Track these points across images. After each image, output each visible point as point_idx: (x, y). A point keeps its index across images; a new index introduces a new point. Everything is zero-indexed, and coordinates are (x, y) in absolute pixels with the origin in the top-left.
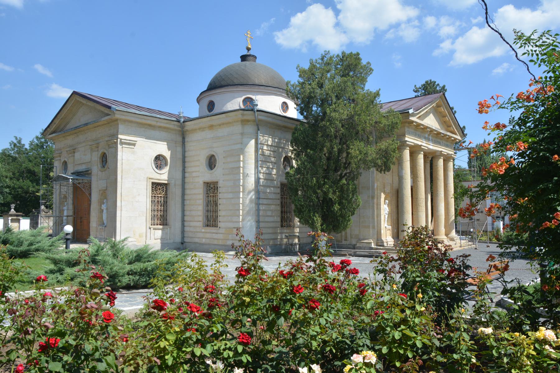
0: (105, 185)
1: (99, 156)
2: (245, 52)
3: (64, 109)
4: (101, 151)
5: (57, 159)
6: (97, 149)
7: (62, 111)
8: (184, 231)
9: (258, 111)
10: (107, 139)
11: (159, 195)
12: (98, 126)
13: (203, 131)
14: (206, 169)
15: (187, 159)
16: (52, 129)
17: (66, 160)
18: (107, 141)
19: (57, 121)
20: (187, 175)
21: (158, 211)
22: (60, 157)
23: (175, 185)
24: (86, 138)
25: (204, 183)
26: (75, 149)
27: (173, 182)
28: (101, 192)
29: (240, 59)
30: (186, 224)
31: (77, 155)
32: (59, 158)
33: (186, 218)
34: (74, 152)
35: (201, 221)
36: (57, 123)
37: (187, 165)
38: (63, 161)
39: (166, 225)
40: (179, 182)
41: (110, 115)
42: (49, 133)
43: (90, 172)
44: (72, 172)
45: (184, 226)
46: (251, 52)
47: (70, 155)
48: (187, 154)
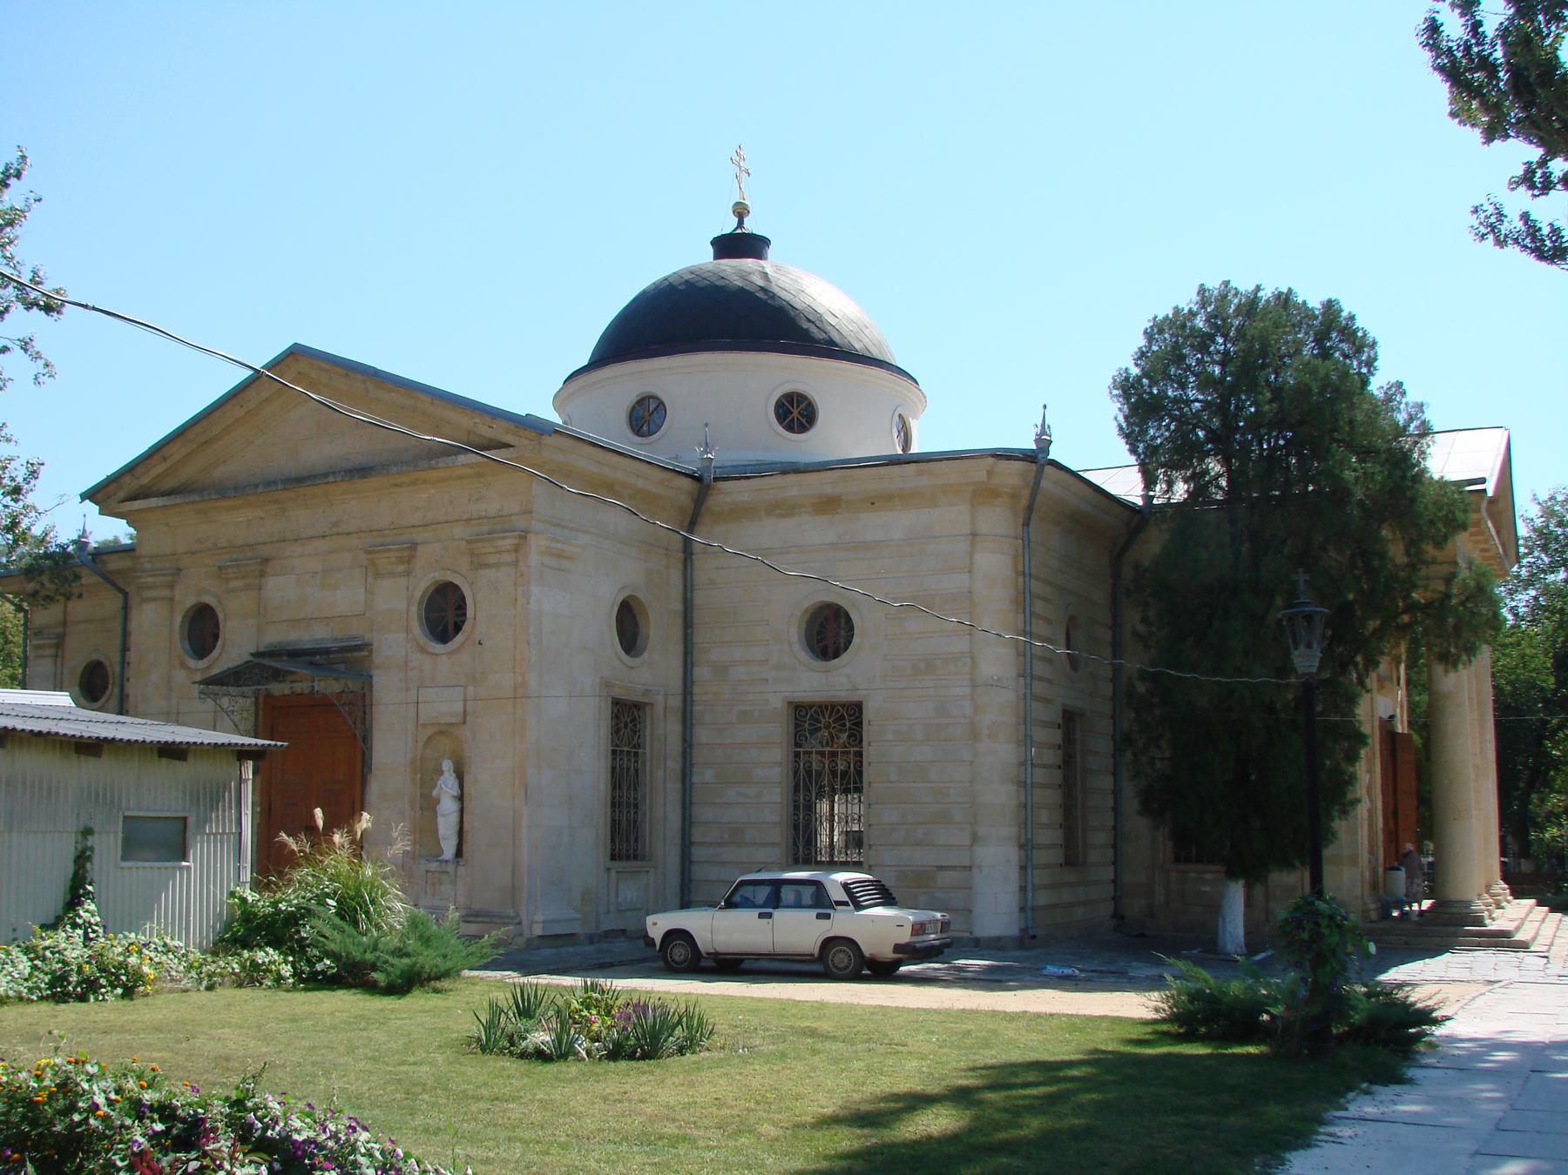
0: (459, 707)
1: (418, 595)
2: (728, 225)
3: (228, 406)
4: (423, 583)
5: (149, 594)
6: (402, 568)
7: (217, 414)
8: (690, 880)
9: (1054, 463)
10: (460, 531)
11: (626, 749)
12: (413, 483)
13: (783, 516)
14: (804, 655)
15: (697, 615)
16: (145, 480)
17: (208, 599)
18: (470, 542)
19: (178, 453)
20: (701, 673)
21: (628, 805)
22: (171, 586)
23: (666, 707)
24: (335, 524)
25: (790, 703)
26: (266, 560)
27: (660, 699)
28: (430, 731)
29: (710, 251)
30: (697, 853)
31: (279, 588)
32: (165, 593)
33: (697, 835)
34: (262, 574)
35: (773, 844)
36: (176, 458)
37: (701, 637)
38: (190, 601)
39: (636, 858)
40: (675, 702)
41: (507, 446)
42: (122, 495)
43: (365, 653)
44: (253, 651)
45: (691, 862)
46: (752, 226)
47: (235, 584)
48: (700, 598)
